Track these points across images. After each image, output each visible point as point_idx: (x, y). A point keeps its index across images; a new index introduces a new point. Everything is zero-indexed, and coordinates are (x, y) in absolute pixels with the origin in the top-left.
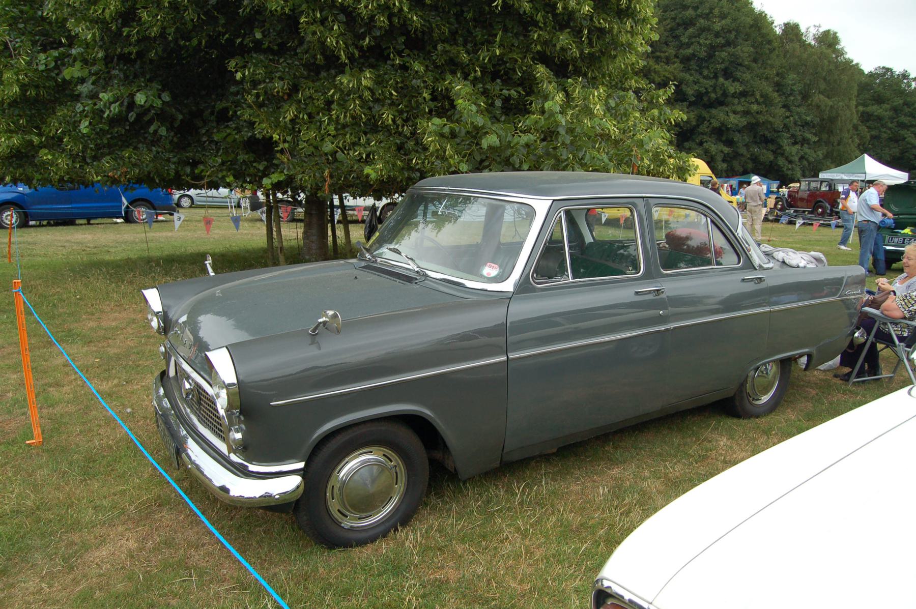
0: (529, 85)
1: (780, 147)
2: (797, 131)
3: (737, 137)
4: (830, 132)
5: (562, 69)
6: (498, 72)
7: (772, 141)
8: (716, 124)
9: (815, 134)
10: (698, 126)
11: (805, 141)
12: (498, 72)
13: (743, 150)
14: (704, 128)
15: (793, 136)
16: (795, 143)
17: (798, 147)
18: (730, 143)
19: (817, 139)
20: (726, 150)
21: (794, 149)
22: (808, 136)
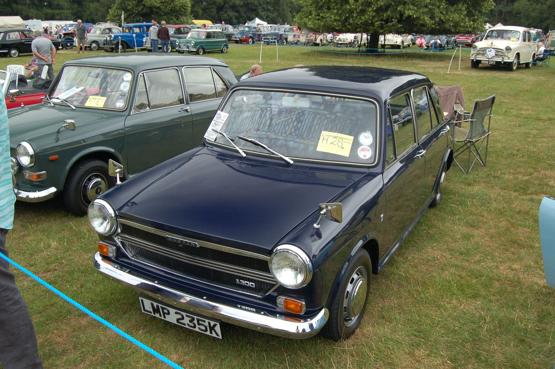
0: (179, 17)
1: (258, 13)
2: (265, 6)
3: (240, 9)
4: (279, 6)
5: (181, 15)
6: (176, 16)
7: (255, 10)
8: (231, 4)
9: (272, 7)
10: (225, 4)
11: (268, 10)
12: (176, 16)
13: (243, 14)
14: (227, 6)
15: (263, 8)
16: (264, 11)
17: (265, 12)
18: (238, 12)
19: (273, 9)
20: (236, 14)
21: (263, 13)
22: (269, 7)
